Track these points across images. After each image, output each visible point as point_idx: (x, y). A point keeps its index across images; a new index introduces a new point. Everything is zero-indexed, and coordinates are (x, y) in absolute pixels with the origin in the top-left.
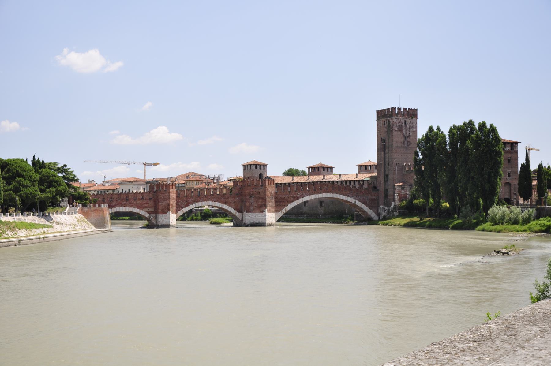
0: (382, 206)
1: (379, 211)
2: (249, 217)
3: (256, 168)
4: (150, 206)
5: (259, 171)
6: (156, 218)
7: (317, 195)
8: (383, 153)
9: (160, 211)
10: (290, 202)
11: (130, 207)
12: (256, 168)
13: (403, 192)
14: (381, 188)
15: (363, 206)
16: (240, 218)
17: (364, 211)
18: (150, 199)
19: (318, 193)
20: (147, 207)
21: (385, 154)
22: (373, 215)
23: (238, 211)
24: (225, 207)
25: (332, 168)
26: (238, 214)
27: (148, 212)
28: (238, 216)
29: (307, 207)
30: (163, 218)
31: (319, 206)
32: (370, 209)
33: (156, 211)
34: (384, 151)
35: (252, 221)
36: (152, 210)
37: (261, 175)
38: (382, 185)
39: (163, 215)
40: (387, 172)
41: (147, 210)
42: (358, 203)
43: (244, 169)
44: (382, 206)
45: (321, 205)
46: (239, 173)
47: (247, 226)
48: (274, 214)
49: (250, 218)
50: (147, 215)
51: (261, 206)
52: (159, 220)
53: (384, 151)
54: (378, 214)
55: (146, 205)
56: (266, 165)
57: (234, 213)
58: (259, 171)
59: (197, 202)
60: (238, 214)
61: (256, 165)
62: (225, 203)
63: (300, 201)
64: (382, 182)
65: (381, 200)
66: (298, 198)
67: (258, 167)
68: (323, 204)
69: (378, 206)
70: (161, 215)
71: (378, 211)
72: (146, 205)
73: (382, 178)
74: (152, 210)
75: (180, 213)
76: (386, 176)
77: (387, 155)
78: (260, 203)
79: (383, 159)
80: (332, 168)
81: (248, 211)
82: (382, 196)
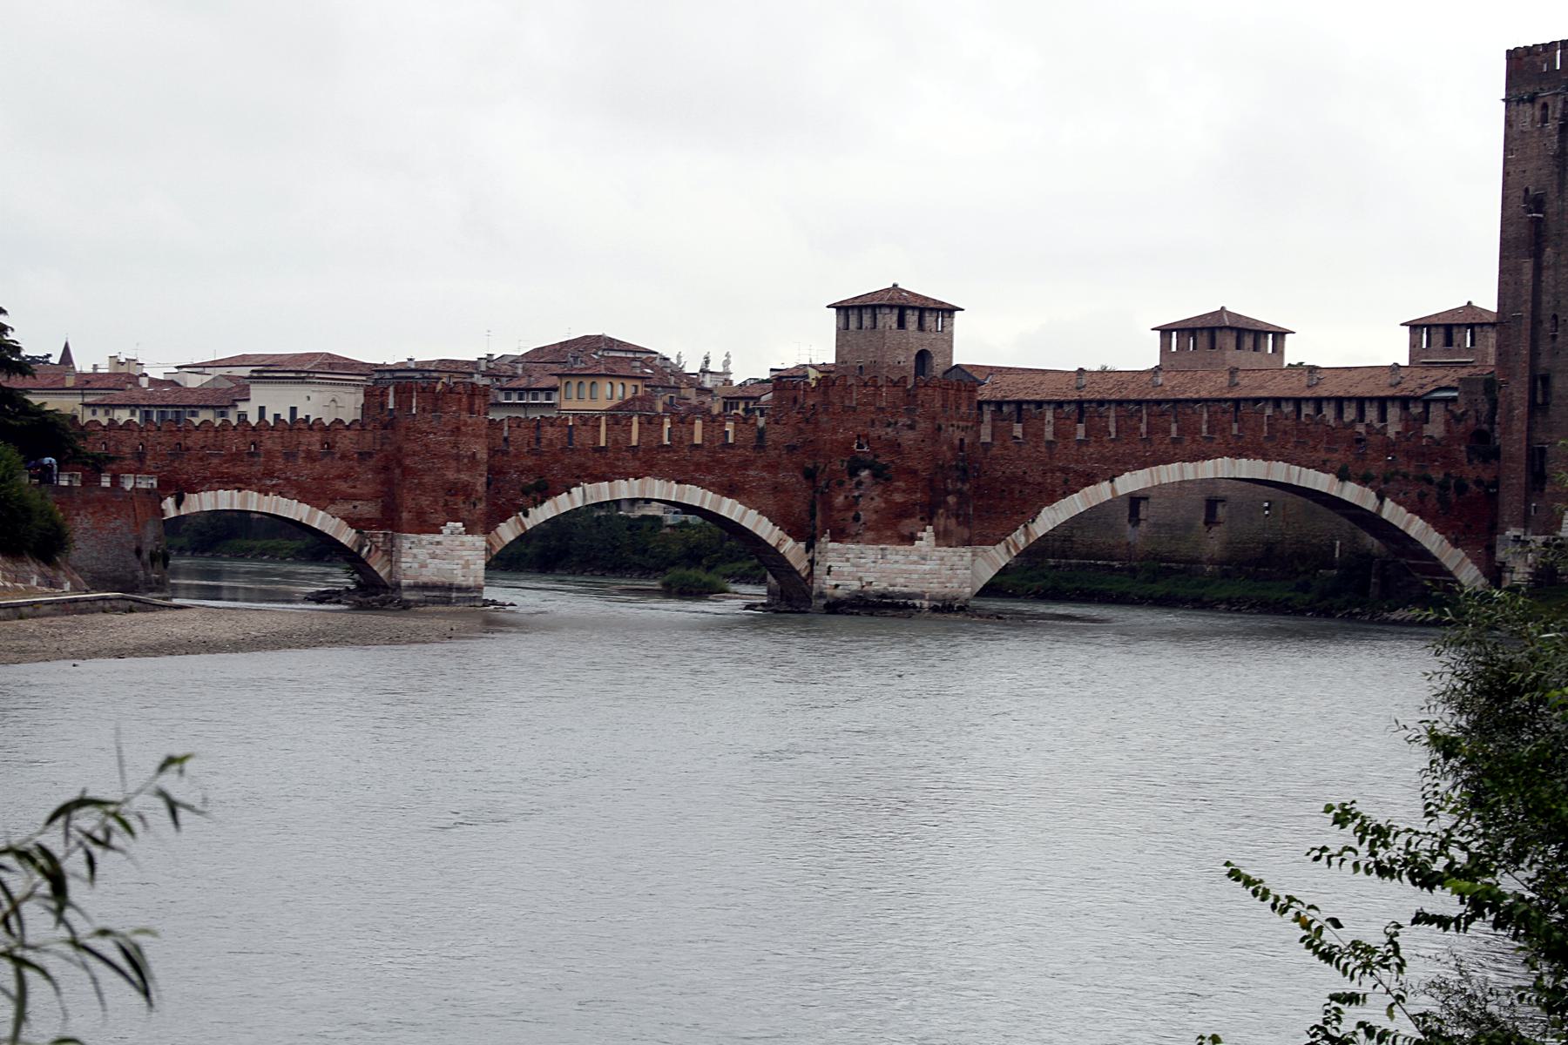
1: (1500, 555)
2: (850, 566)
3: (901, 324)
4: (362, 489)
5: (914, 339)
6: (390, 554)
7: (1189, 467)
8: (1528, 266)
10: (1052, 498)
11: (264, 491)
12: (901, 324)
14: (1513, 442)
15: (1416, 527)
16: (801, 566)
17: (1426, 554)
18: (364, 456)
19: (1194, 458)
20: (347, 498)
21: (1538, 269)
22: (1469, 575)
24: (730, 509)
25: (1280, 335)
26: (791, 549)
27: (352, 522)
28: (790, 558)
29: (1143, 526)
30: (422, 553)
31: (1201, 523)
32: (1455, 544)
33: (392, 517)
34: (1537, 255)
35: (856, 585)
37: (923, 357)
38: (1519, 426)
39: (426, 537)
40: (1544, 362)
41: (347, 507)
42: (1392, 512)
43: (843, 330)
44: (1512, 532)
45: (1211, 520)
46: (815, 345)
47: (837, 607)
48: (967, 552)
49: (847, 568)
50: (347, 537)
51: (903, 512)
53: (1537, 255)
54: (1495, 573)
55: (343, 486)
56: (950, 311)
57: (772, 542)
58: (914, 339)
59: (595, 478)
60: (791, 549)
61: (902, 310)
62: (730, 490)
63: (1101, 492)
64: (1521, 410)
65: (1510, 501)
66: (1090, 479)
67: (912, 318)
68: (1221, 511)
69: (1494, 528)
70: (414, 537)
71: (1491, 550)
72: (343, 486)
73: (1517, 392)
74: (367, 509)
75: (507, 532)
76: (1540, 381)
77: (1548, 277)
78: (898, 498)
79: (1527, 295)
80: (1280, 335)
81: (839, 535)
82: (1515, 476)
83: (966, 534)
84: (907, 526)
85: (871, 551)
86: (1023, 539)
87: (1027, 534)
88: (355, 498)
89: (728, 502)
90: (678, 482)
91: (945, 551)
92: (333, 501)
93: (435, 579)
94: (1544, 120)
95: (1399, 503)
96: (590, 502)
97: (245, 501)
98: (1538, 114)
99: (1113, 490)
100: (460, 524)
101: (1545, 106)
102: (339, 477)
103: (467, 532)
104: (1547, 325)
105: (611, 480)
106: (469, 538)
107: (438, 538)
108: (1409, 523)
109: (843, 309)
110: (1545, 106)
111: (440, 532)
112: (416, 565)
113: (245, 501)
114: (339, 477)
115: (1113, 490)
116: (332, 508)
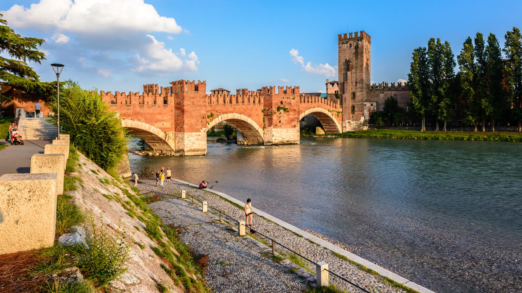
0: (347, 121)
1: (344, 125)
9: (185, 126)
13: (372, 107)
20: (160, 121)
27: (162, 129)
30: (193, 139)
36: (169, 124)
39: (194, 134)
41: (160, 124)
49: (278, 135)
52: (186, 142)
55: (159, 117)
59: (224, 113)
62: (250, 116)
70: (189, 133)
72: (159, 117)
78: (291, 117)
84: (294, 123)
85: (284, 130)
88: (163, 121)
89: (249, 119)
93: (198, 148)
94: (351, 46)
98: (349, 45)
101: (351, 44)
102: (157, 114)
104: (355, 84)
105: (227, 113)
107: (199, 133)
110: (351, 44)
111: (200, 131)
112: (190, 143)
114: (157, 114)
116: (156, 125)
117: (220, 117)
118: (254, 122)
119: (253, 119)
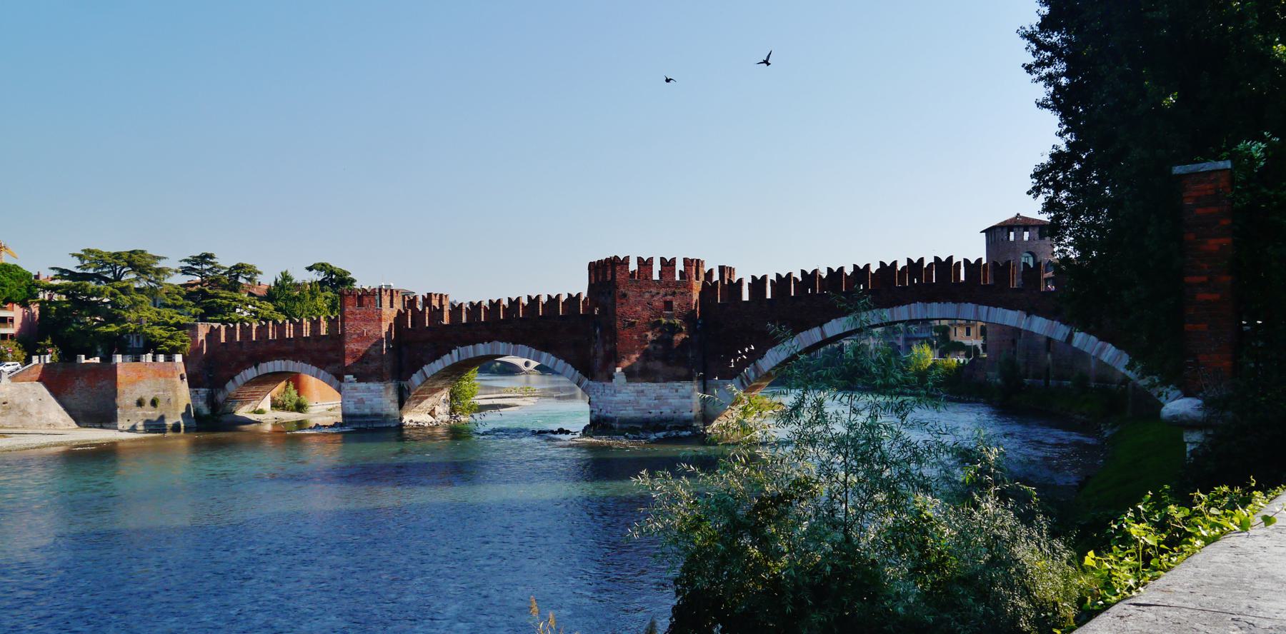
23: (586, 376)
59: (465, 343)
83: (683, 371)
86: (753, 374)
87: (756, 370)
90: (514, 343)
91: (652, 389)
92: (328, 364)
95: (1090, 333)
96: (463, 358)
97: (287, 366)
99: (823, 333)
100: (350, 377)
103: (359, 381)
105: (474, 344)
106: (363, 385)
108: (1101, 350)
109: (988, 232)
113: (287, 366)
115: (823, 333)
117: (455, 352)
118: (561, 362)
119: (559, 356)
